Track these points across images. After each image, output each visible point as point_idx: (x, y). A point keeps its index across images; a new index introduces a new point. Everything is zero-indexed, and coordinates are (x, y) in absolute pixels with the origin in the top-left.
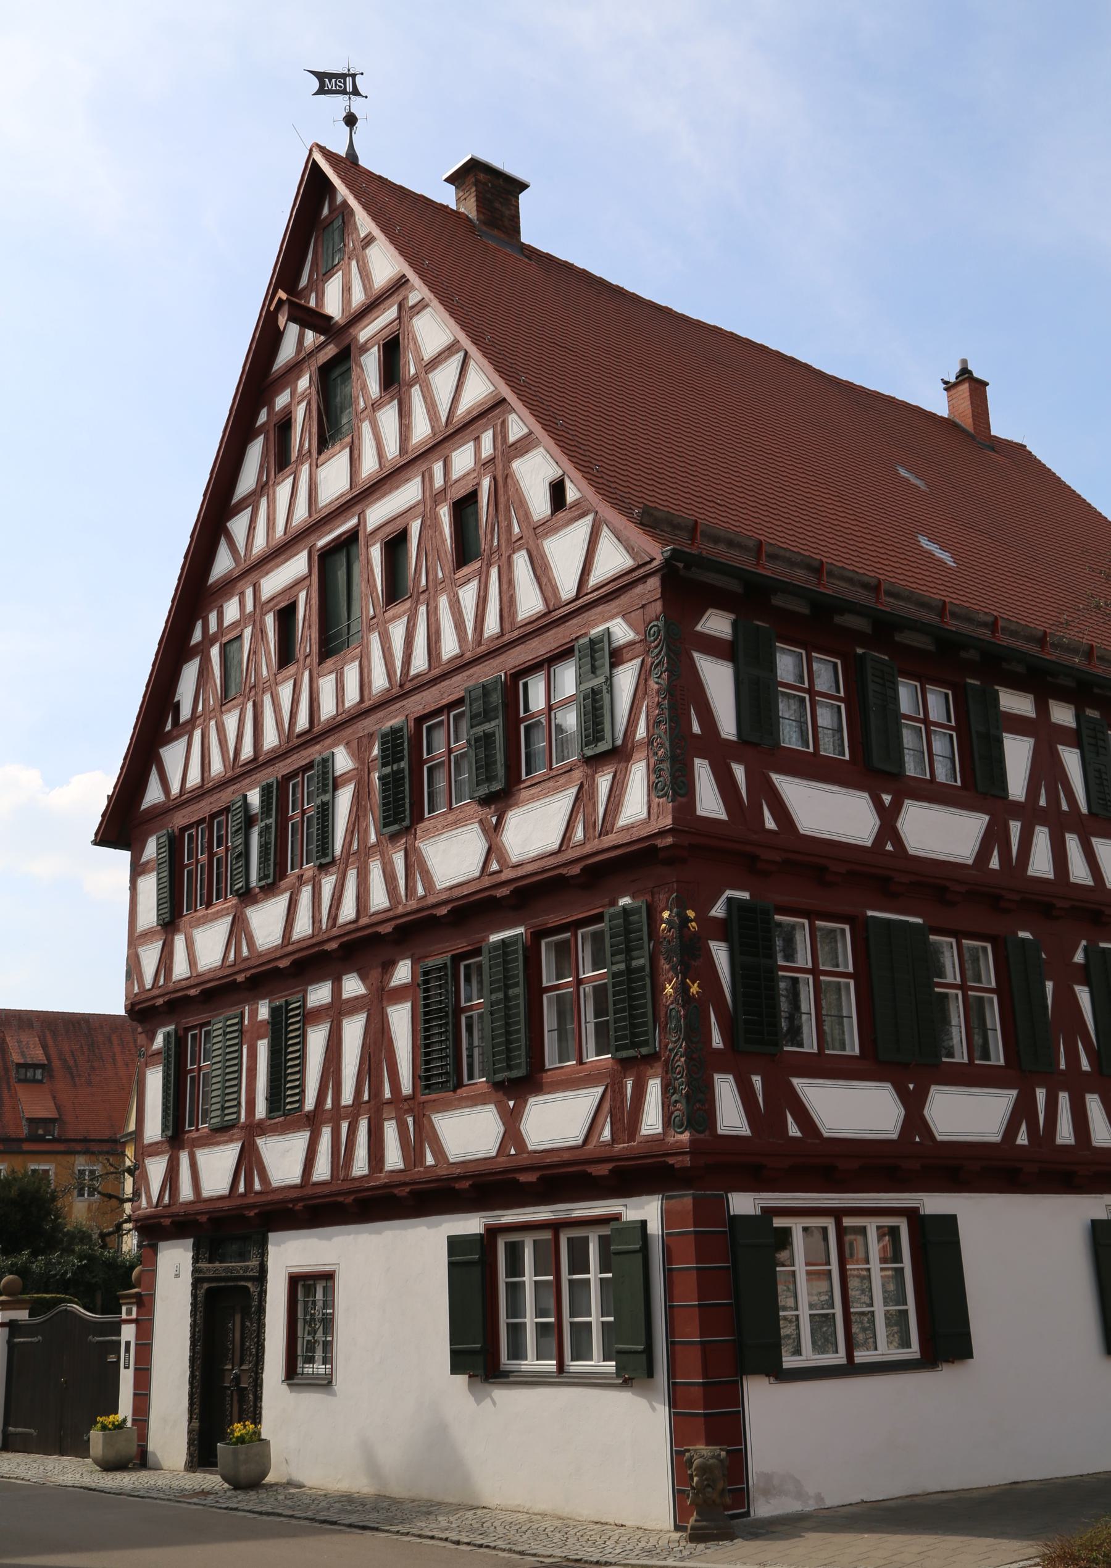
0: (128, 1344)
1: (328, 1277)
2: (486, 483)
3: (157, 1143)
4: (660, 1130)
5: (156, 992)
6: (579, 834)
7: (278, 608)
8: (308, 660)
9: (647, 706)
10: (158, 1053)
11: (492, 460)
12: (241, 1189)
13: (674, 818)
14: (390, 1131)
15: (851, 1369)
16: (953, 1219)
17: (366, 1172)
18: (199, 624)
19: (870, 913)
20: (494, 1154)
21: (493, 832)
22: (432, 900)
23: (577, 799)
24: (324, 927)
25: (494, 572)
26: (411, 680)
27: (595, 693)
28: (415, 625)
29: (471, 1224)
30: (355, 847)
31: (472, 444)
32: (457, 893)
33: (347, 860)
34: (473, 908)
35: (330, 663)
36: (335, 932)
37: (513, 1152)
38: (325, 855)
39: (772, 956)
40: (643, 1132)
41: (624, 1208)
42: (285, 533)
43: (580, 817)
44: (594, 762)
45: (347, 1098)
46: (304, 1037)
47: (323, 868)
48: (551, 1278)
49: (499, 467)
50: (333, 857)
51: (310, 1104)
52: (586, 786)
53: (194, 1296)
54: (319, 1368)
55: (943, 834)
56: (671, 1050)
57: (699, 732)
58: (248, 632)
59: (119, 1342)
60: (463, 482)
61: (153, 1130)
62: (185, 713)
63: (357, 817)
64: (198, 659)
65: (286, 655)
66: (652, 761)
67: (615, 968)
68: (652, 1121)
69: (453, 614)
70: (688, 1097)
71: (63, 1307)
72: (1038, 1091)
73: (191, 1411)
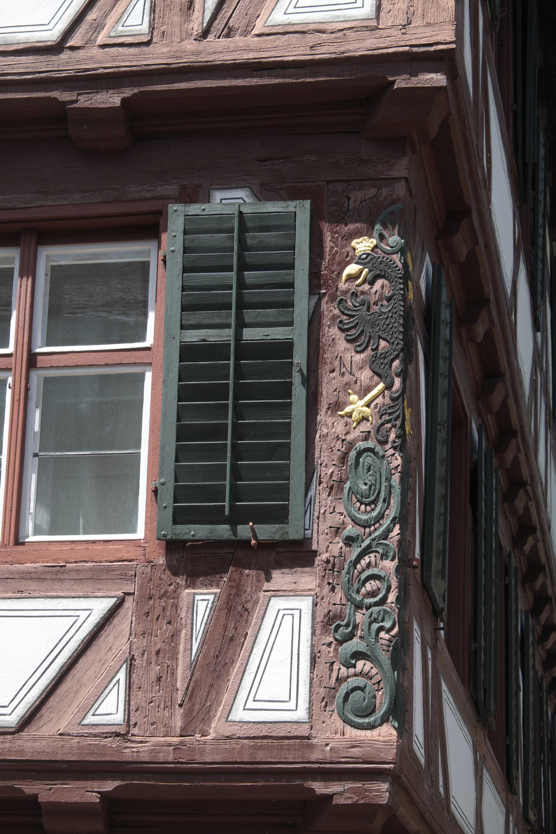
4: (301, 714)
56: (350, 541)
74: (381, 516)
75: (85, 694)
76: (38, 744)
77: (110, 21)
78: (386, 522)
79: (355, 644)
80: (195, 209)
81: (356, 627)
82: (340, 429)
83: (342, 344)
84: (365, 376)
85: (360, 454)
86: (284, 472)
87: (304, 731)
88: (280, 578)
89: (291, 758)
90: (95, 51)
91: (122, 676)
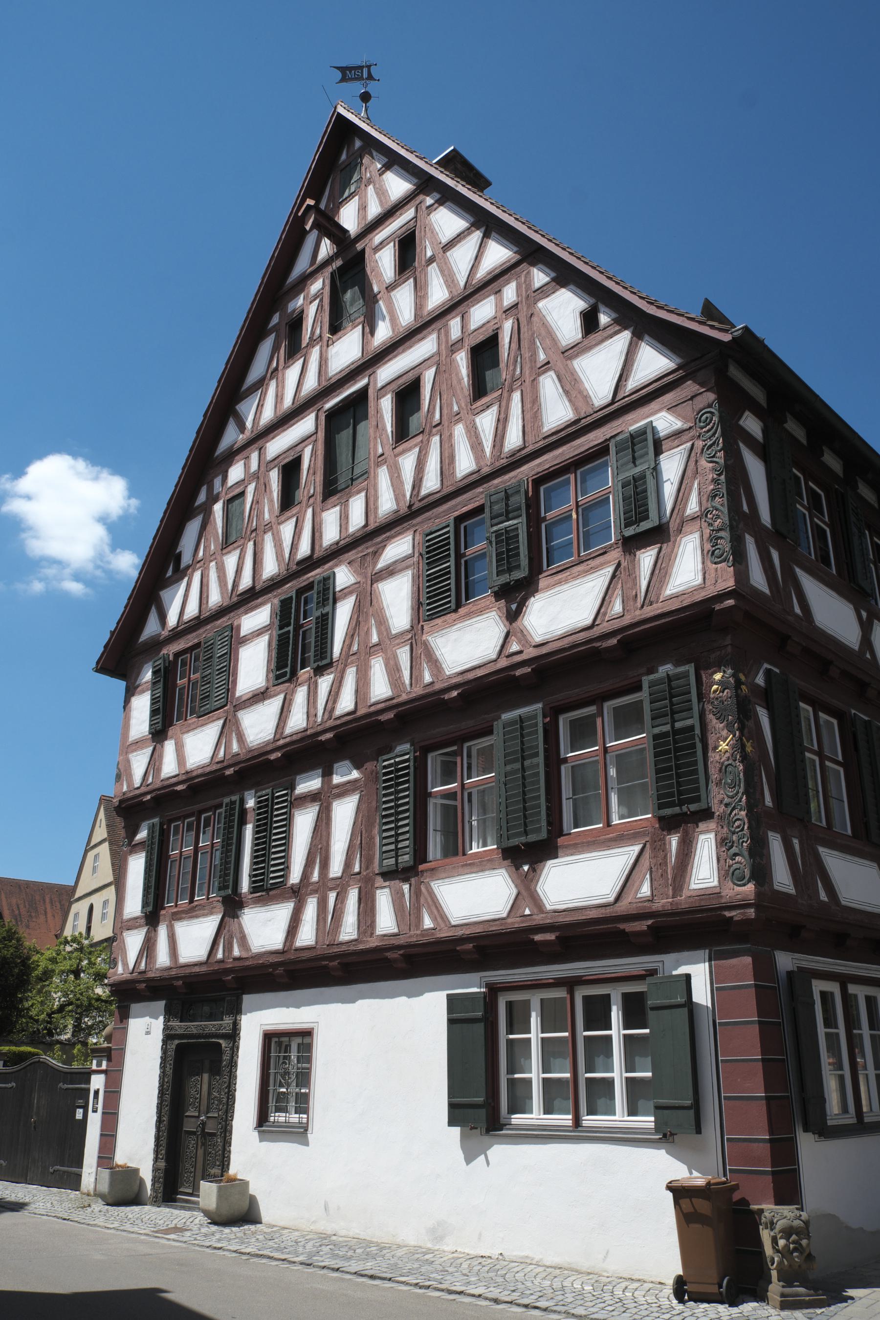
0: (97, 1093)
1: (307, 1033)
3: (136, 918)
4: (716, 883)
6: (617, 607)
7: (282, 464)
8: (312, 500)
9: (699, 484)
10: (142, 843)
11: (515, 306)
12: (220, 955)
13: (736, 581)
14: (384, 900)
17: (354, 936)
21: (513, 616)
22: (438, 686)
23: (614, 576)
24: (319, 720)
25: (516, 396)
26: (420, 501)
27: (638, 481)
28: (426, 454)
29: (472, 986)
30: (355, 648)
31: (492, 297)
32: (471, 676)
33: (346, 660)
34: (487, 691)
35: (333, 499)
37: (527, 912)
40: (693, 886)
41: (660, 965)
42: (293, 403)
43: (619, 592)
44: (631, 545)
45: (336, 868)
47: (319, 671)
48: (566, 1034)
49: (523, 311)
50: (332, 659)
52: (624, 564)
53: (164, 1051)
54: (294, 1118)
56: (727, 805)
59: (88, 1090)
60: (484, 329)
62: (186, 560)
63: (358, 623)
64: (202, 516)
65: (288, 501)
66: (707, 532)
67: (657, 730)
69: (469, 438)
73: (157, 1152)
74: (738, 792)
75: (636, 885)
76: (623, 907)
77: (609, 611)
78: (740, 795)
79: (734, 850)
80: (652, 677)
81: (733, 842)
82: (718, 757)
83: (715, 721)
84: (725, 733)
85: (726, 767)
86: (697, 781)
87: (718, 890)
88: (702, 826)
89: (714, 903)
90: (605, 624)
91: (648, 876)
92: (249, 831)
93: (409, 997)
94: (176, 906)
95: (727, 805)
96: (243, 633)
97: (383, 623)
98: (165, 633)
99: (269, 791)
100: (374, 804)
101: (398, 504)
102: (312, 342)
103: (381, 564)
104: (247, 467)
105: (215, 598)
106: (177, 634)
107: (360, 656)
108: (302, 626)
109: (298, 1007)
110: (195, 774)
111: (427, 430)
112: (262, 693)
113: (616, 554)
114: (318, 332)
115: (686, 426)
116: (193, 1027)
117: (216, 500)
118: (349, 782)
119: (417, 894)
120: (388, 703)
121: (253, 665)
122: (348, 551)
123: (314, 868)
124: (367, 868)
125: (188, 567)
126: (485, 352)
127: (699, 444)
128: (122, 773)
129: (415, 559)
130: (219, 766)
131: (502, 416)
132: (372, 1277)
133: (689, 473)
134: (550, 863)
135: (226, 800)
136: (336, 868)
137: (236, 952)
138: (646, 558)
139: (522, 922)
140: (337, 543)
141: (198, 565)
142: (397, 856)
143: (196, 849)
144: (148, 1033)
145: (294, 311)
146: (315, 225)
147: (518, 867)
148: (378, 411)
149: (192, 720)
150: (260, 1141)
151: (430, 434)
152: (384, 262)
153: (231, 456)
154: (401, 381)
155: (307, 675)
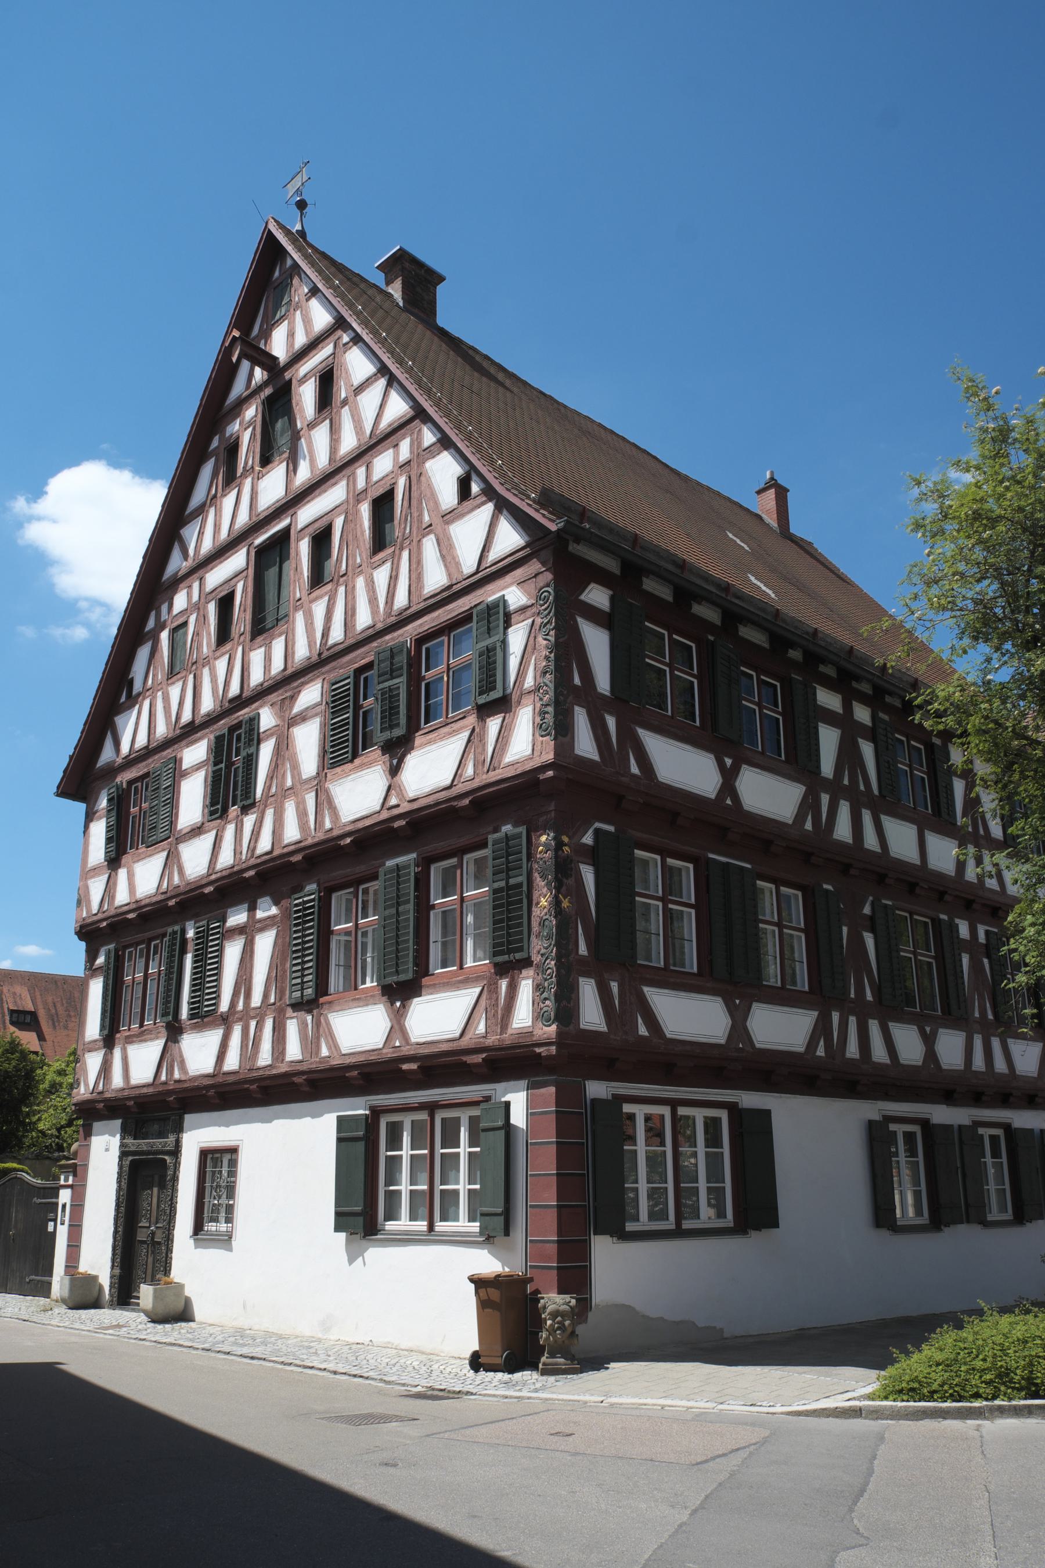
0: (64, 1206)
1: (233, 1151)
2: (402, 482)
3: (95, 1041)
4: (530, 1024)
5: (100, 916)
6: (469, 771)
11: (408, 463)
12: (163, 1078)
13: (555, 754)
14: (292, 1028)
15: (679, 1233)
16: (767, 1113)
17: (269, 1062)
18: (153, 614)
19: (711, 856)
20: (381, 1046)
21: (394, 771)
22: (336, 833)
23: (469, 741)
24: (244, 857)
25: (405, 554)
26: (328, 650)
27: (490, 651)
28: (334, 603)
29: (357, 1108)
30: (273, 790)
31: (391, 451)
32: (360, 825)
33: (266, 801)
34: (374, 839)
35: (260, 639)
36: (253, 862)
37: (397, 1044)
38: (247, 798)
39: (632, 884)
40: (515, 1026)
43: (471, 756)
44: (484, 711)
45: (256, 1000)
46: (221, 951)
47: (245, 810)
48: (426, 1152)
49: (413, 468)
51: (224, 1006)
52: (477, 730)
53: (121, 1166)
54: (223, 1227)
55: (769, 795)
56: (542, 955)
57: (579, 684)
58: (192, 619)
59: (57, 1204)
60: (383, 482)
61: (93, 1028)
62: (137, 687)
63: (277, 766)
65: (223, 636)
66: (538, 705)
67: (496, 885)
68: (523, 1016)
69: (368, 592)
70: (556, 995)
71: (13, 1175)
72: (834, 1013)
73: (113, 1261)
76: (465, 1043)
79: (545, 995)
83: (539, 879)
84: (545, 890)
86: (521, 933)
89: (528, 1041)
90: (460, 785)
92: (189, 959)
93: (313, 1117)
94: (129, 1029)
95: (542, 955)
96: (184, 767)
97: (295, 767)
98: (119, 760)
99: (204, 922)
100: (288, 939)
101: (310, 651)
102: (244, 475)
103: (297, 708)
104: (189, 596)
105: (162, 730)
106: (130, 762)
107: (277, 798)
108: (233, 763)
109: (228, 1126)
110: (143, 903)
111: (335, 579)
112: (199, 828)
113: (472, 719)
114: (250, 462)
115: (529, 603)
116: (143, 1144)
117: (163, 628)
118: (269, 917)
119: (317, 1024)
120: (297, 846)
121: (192, 799)
122: (270, 694)
123: (239, 998)
124: (281, 999)
125: (139, 694)
126: (383, 505)
127: (539, 621)
128: (82, 900)
129: (323, 707)
130: (163, 897)
131: (394, 573)
132: (252, 1358)
133: (529, 648)
134: (416, 1000)
135: (170, 930)
136: (256, 1000)
137: (177, 1075)
138: (493, 725)
139: (393, 1053)
140: (262, 685)
141: (148, 694)
142: (302, 989)
143: (146, 976)
144: (107, 1150)
145: (232, 435)
146: (242, 355)
147: (392, 1004)
148: (297, 554)
149: (142, 849)
150: (196, 1248)
151: (338, 584)
152: (306, 395)
153: (176, 582)
154: (317, 525)
155: (235, 814)
